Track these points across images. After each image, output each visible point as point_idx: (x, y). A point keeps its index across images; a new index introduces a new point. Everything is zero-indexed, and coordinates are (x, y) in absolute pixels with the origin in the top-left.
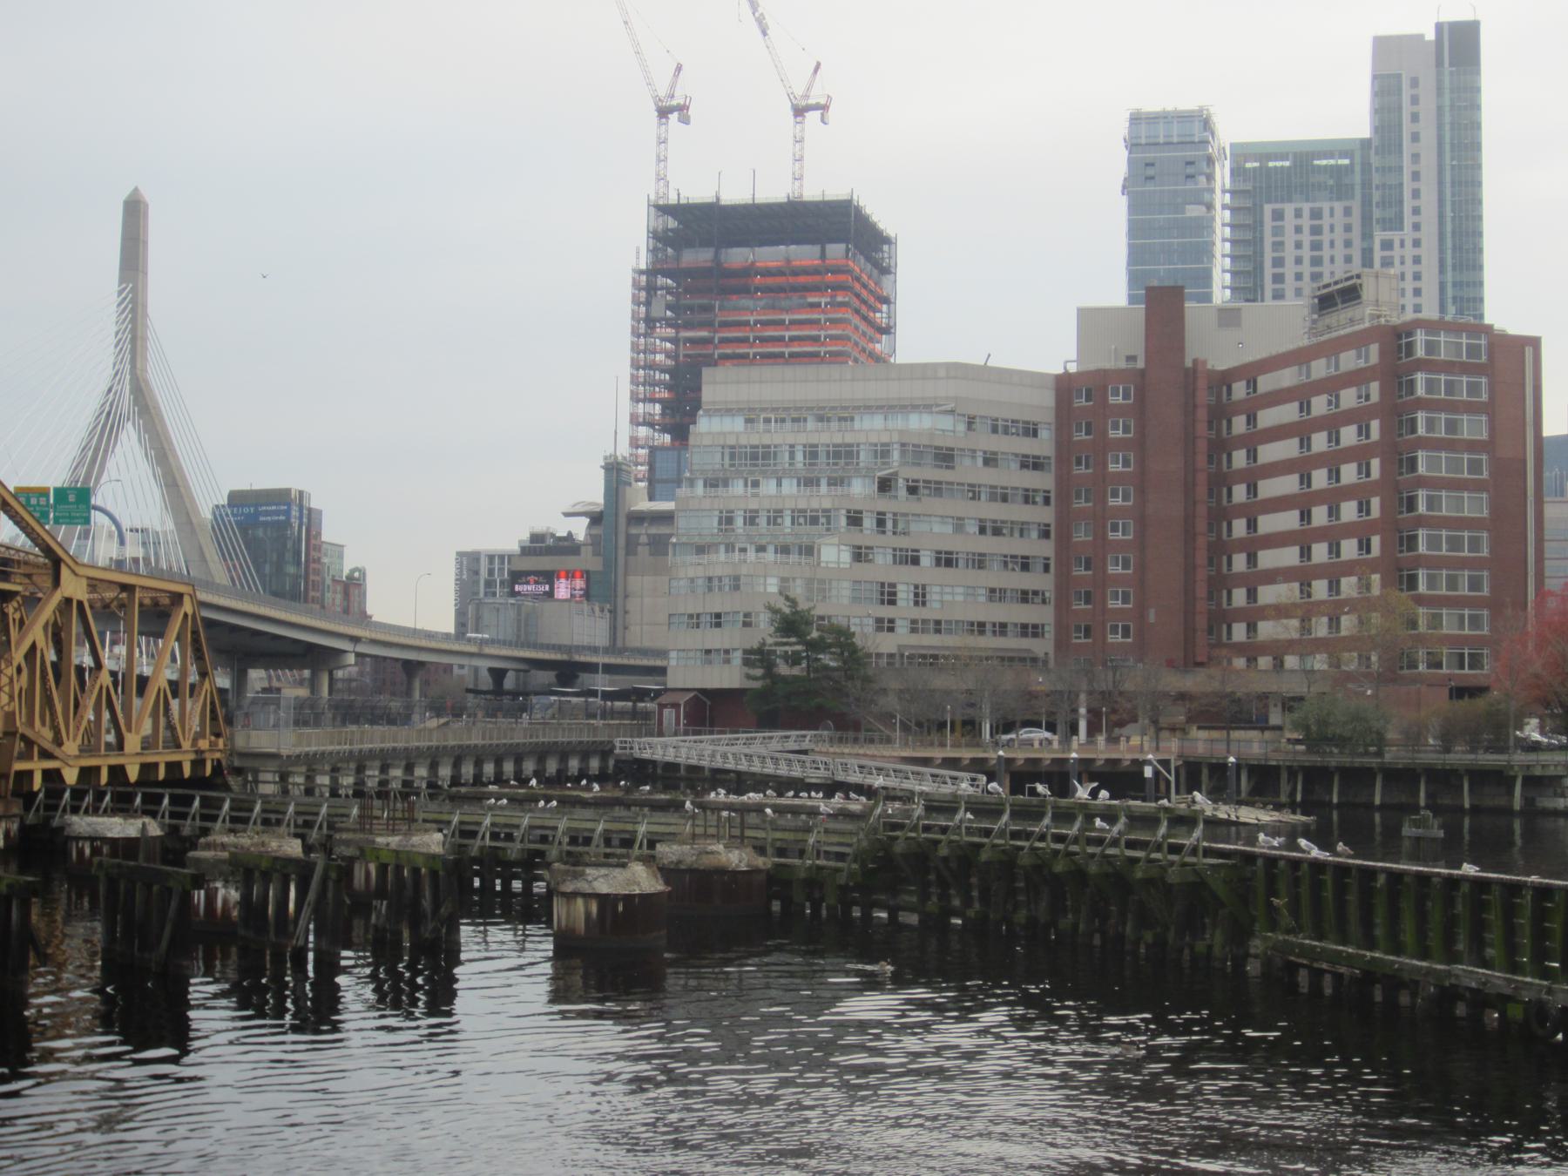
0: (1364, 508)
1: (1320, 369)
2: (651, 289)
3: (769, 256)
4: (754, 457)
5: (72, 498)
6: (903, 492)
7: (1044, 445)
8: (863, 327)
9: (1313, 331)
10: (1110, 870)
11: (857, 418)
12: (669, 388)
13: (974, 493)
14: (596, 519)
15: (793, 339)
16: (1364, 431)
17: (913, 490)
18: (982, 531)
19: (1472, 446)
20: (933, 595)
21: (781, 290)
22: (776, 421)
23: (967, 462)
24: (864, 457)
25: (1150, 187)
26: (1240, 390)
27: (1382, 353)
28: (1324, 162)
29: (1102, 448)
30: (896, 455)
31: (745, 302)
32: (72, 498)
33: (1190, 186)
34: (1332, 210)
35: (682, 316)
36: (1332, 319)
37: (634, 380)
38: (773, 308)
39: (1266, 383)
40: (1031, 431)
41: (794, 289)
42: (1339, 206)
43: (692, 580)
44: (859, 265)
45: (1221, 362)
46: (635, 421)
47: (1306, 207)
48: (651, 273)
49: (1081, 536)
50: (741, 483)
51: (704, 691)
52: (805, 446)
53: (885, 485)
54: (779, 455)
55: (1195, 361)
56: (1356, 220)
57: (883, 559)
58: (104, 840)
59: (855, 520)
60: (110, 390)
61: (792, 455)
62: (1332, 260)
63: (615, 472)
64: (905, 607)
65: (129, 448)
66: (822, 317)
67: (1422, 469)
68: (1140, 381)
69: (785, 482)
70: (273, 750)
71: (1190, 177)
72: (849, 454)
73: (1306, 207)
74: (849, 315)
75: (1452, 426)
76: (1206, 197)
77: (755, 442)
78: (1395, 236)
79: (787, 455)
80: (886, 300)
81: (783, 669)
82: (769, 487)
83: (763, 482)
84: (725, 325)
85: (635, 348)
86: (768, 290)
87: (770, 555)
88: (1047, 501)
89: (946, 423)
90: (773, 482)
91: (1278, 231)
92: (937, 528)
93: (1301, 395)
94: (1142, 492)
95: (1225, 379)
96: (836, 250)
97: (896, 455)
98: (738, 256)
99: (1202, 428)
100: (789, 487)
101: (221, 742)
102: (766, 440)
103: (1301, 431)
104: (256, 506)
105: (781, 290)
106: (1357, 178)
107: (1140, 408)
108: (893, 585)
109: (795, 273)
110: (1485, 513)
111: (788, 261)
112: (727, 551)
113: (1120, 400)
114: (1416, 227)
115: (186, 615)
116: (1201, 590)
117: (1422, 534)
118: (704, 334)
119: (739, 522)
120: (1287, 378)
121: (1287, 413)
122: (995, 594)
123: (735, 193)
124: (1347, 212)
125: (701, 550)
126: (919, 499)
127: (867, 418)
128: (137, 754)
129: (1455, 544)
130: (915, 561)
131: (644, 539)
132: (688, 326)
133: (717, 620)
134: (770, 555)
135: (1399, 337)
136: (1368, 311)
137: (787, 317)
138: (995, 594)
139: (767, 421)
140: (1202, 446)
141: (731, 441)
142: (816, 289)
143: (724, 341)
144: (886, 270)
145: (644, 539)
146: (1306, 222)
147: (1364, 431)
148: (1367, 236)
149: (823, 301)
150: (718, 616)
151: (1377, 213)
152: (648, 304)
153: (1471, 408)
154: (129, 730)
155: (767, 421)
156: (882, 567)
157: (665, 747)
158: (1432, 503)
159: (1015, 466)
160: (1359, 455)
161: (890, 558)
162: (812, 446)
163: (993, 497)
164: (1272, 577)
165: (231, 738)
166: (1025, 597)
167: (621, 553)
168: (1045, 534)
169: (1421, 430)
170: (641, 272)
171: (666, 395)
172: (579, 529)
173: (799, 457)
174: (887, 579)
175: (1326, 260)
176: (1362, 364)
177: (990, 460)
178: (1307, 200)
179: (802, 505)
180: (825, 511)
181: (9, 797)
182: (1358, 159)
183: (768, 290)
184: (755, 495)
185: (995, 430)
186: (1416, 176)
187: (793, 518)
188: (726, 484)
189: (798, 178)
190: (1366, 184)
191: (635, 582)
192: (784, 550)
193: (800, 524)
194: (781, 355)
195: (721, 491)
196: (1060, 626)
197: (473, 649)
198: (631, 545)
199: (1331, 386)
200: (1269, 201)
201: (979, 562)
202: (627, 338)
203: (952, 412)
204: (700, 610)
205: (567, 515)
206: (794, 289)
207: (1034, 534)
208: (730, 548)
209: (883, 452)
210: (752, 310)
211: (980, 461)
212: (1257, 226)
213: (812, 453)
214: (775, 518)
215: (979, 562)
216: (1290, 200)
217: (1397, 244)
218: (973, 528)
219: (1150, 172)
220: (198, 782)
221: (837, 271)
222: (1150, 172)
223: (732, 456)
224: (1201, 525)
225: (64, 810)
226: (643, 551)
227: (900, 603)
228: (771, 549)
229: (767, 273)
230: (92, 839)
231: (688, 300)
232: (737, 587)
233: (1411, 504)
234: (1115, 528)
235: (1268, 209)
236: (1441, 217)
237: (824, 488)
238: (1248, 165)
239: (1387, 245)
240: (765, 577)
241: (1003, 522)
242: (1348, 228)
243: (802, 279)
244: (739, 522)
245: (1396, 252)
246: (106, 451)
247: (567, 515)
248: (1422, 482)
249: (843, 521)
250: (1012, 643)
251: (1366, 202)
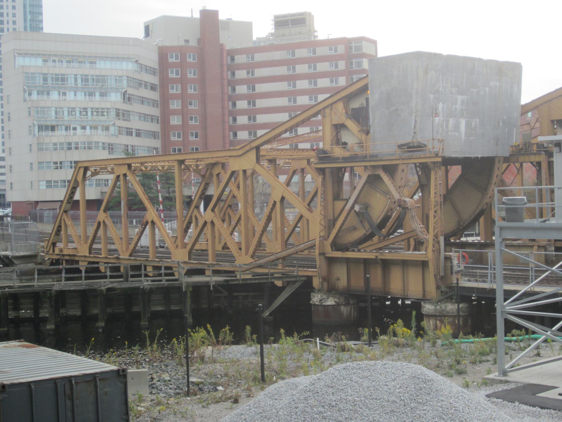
10: (324, 230)
11: (98, 62)
22: (59, 62)
24: (111, 83)
54: (69, 79)
61: (76, 80)
72: (63, 80)
77: (58, 72)
79: (73, 79)
82: (70, 96)
83: (68, 93)
97: (125, 82)
100: (80, 96)
102: (63, 72)
126: (131, 104)
127: (102, 63)
155: (54, 61)
162: (85, 75)
173: (79, 81)
180: (108, 109)
187: (68, 112)
193: (84, 115)
204: (62, 159)
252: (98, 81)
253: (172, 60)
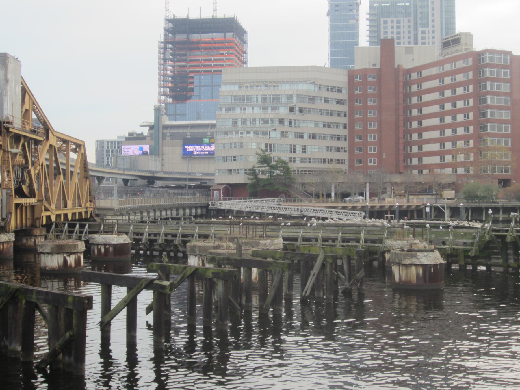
0: (466, 116)
1: (448, 67)
2: (165, 48)
3: (206, 37)
4: (243, 100)
6: (298, 112)
7: (344, 96)
8: (238, 61)
9: (441, 54)
11: (280, 85)
12: (172, 83)
13: (321, 112)
14: (151, 127)
15: (215, 66)
16: (466, 89)
17: (301, 111)
18: (324, 126)
19: (505, 94)
20: (308, 149)
21: (210, 49)
22: (250, 87)
23: (319, 101)
24: (284, 100)
25: (337, 14)
26: (414, 76)
27: (474, 61)
28: (400, 4)
29: (365, 96)
30: (295, 99)
31: (198, 53)
33: (351, 13)
34: (404, 20)
35: (175, 57)
36: (449, 50)
37: (160, 80)
38: (208, 55)
39: (425, 73)
40: (339, 90)
41: (215, 48)
42: (406, 19)
43: (224, 144)
44: (237, 40)
45: (407, 66)
46: (160, 94)
47: (395, 20)
48: (166, 42)
49: (358, 127)
50: (239, 109)
51: (228, 184)
52: (262, 95)
53: (292, 110)
54: (252, 99)
55: (398, 66)
56: (412, 24)
57: (291, 136)
58: (110, 245)
59: (281, 122)
62: (404, 37)
63: (157, 110)
64: (298, 155)
66: (225, 58)
67: (489, 102)
68: (379, 73)
69: (255, 108)
70: (110, 207)
71: (351, 10)
73: (395, 20)
74: (234, 57)
75: (498, 87)
76: (356, 17)
77: (244, 94)
78: (426, 29)
80: (245, 53)
81: (261, 176)
82: (249, 110)
83: (247, 109)
84: (191, 61)
85: (160, 69)
86: (206, 49)
87: (252, 135)
88: (345, 115)
89: (312, 87)
90: (251, 109)
91: (385, 28)
92: (309, 125)
93: (440, 77)
94: (380, 112)
95: (409, 72)
96: (229, 35)
97: (295, 99)
98: (195, 37)
99: (401, 89)
100: (257, 110)
101: (92, 204)
103: (441, 90)
105: (210, 49)
106: (412, 10)
107: (379, 83)
108: (294, 146)
109: (215, 43)
110: (509, 118)
111: (213, 39)
112: (236, 134)
113: (372, 79)
114: (433, 26)
115: (82, 154)
116: (401, 147)
117: (489, 125)
118: (184, 64)
119: (239, 123)
120: (434, 71)
121: (435, 83)
122: (329, 149)
123: (194, 15)
124: (409, 21)
125: (226, 133)
126: (303, 115)
128: (71, 209)
129: (500, 129)
130: (302, 137)
131: (168, 134)
132: (178, 61)
133: (234, 159)
134: (252, 135)
135: (480, 56)
136: (464, 47)
137: (213, 58)
138: (329, 149)
139: (247, 87)
140: (401, 95)
141: (235, 94)
142: (223, 48)
143: (191, 66)
144: (245, 42)
145: (168, 134)
146: (395, 25)
147: (466, 89)
148: (416, 29)
149: (225, 52)
150: (234, 157)
151: (419, 22)
152: (164, 53)
153: (505, 81)
154: (69, 200)
155: (247, 87)
156: (291, 139)
158: (492, 114)
159: (334, 102)
160: (465, 98)
161: (293, 136)
162: (264, 95)
163: (328, 114)
164: (428, 141)
165: (94, 203)
166: (338, 150)
167: (161, 139)
168: (345, 127)
169: (488, 89)
170: (162, 43)
171: (170, 85)
172: (146, 131)
173: (260, 99)
174: (293, 144)
175: (402, 38)
176: (465, 65)
177: (327, 101)
178: (395, 17)
179: (263, 117)
181: (40, 227)
182: (412, 3)
183: (206, 49)
184: (244, 113)
185: (328, 90)
186: (433, 9)
188: (233, 109)
189: (215, 10)
190: (416, 12)
191: (166, 149)
192: (257, 133)
193: (262, 124)
194: (211, 71)
195: (231, 112)
196: (351, 160)
197: (121, 172)
198: (164, 137)
199: (453, 73)
200: (382, 17)
201: (323, 137)
202: (157, 66)
203: (313, 83)
204: (227, 155)
205: (141, 126)
206: (215, 48)
207: (341, 127)
208: (237, 132)
209: (290, 98)
210: (200, 55)
211: (323, 101)
212: (378, 26)
213: (264, 98)
214: (253, 121)
215: (323, 137)
216: (389, 17)
217: (427, 32)
218: (321, 125)
219: (337, 8)
220: (86, 220)
221: (230, 42)
222: (337, 8)
223: (235, 99)
224: (401, 124)
225: (86, 233)
226: (168, 138)
227: (297, 152)
228: (252, 133)
229: (206, 43)
230: (105, 245)
231: (178, 52)
232: (241, 147)
233: (485, 115)
234: (370, 125)
235: (382, 20)
236: (441, 23)
237: (270, 110)
238: (375, 5)
239: (423, 32)
240: (252, 143)
241: (331, 123)
242: (409, 27)
243: (217, 45)
244: (239, 123)
245: (426, 35)
247: (141, 126)
248: (488, 107)
250: (334, 166)
251: (416, 17)
252: (274, 99)
253: (357, 80)
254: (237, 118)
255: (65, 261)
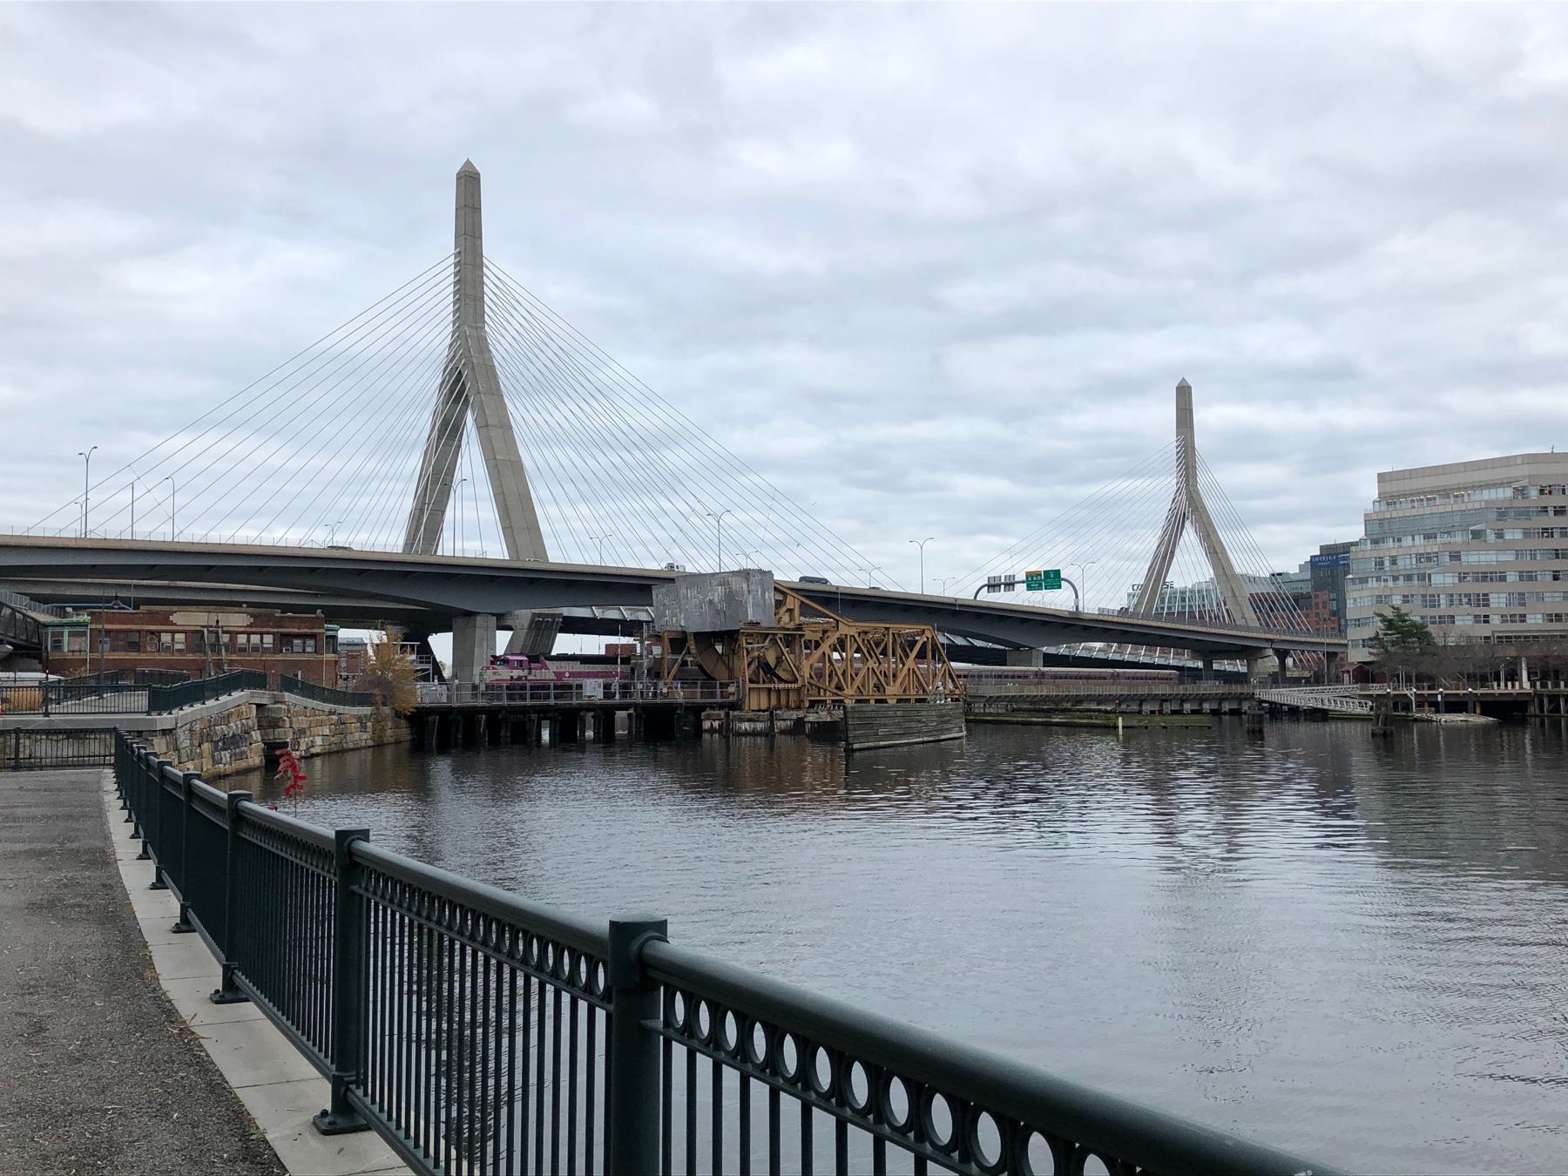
5: (1052, 576)
32: (1052, 576)
60: (1174, 500)
65: (1189, 536)
69: (1416, 537)
82: (1407, 541)
90: (1410, 538)
100: (1419, 540)
104: (1337, 554)
108: (1487, 595)
112: (1377, 581)
119: (1387, 563)
157: (1117, 690)
188: (1383, 540)
208: (1378, 579)
228: (1401, 578)
244: (1387, 563)
246: (1176, 535)
249: (1447, 559)
254: (1382, 555)
255: (712, 725)
